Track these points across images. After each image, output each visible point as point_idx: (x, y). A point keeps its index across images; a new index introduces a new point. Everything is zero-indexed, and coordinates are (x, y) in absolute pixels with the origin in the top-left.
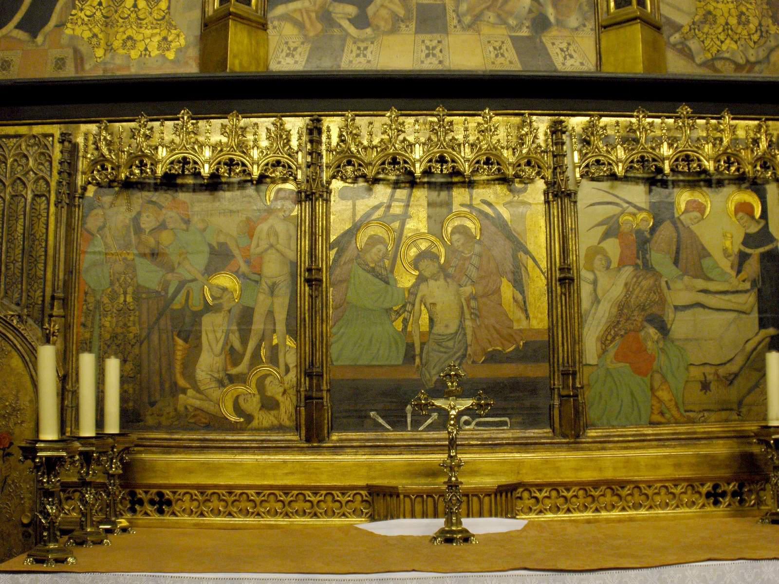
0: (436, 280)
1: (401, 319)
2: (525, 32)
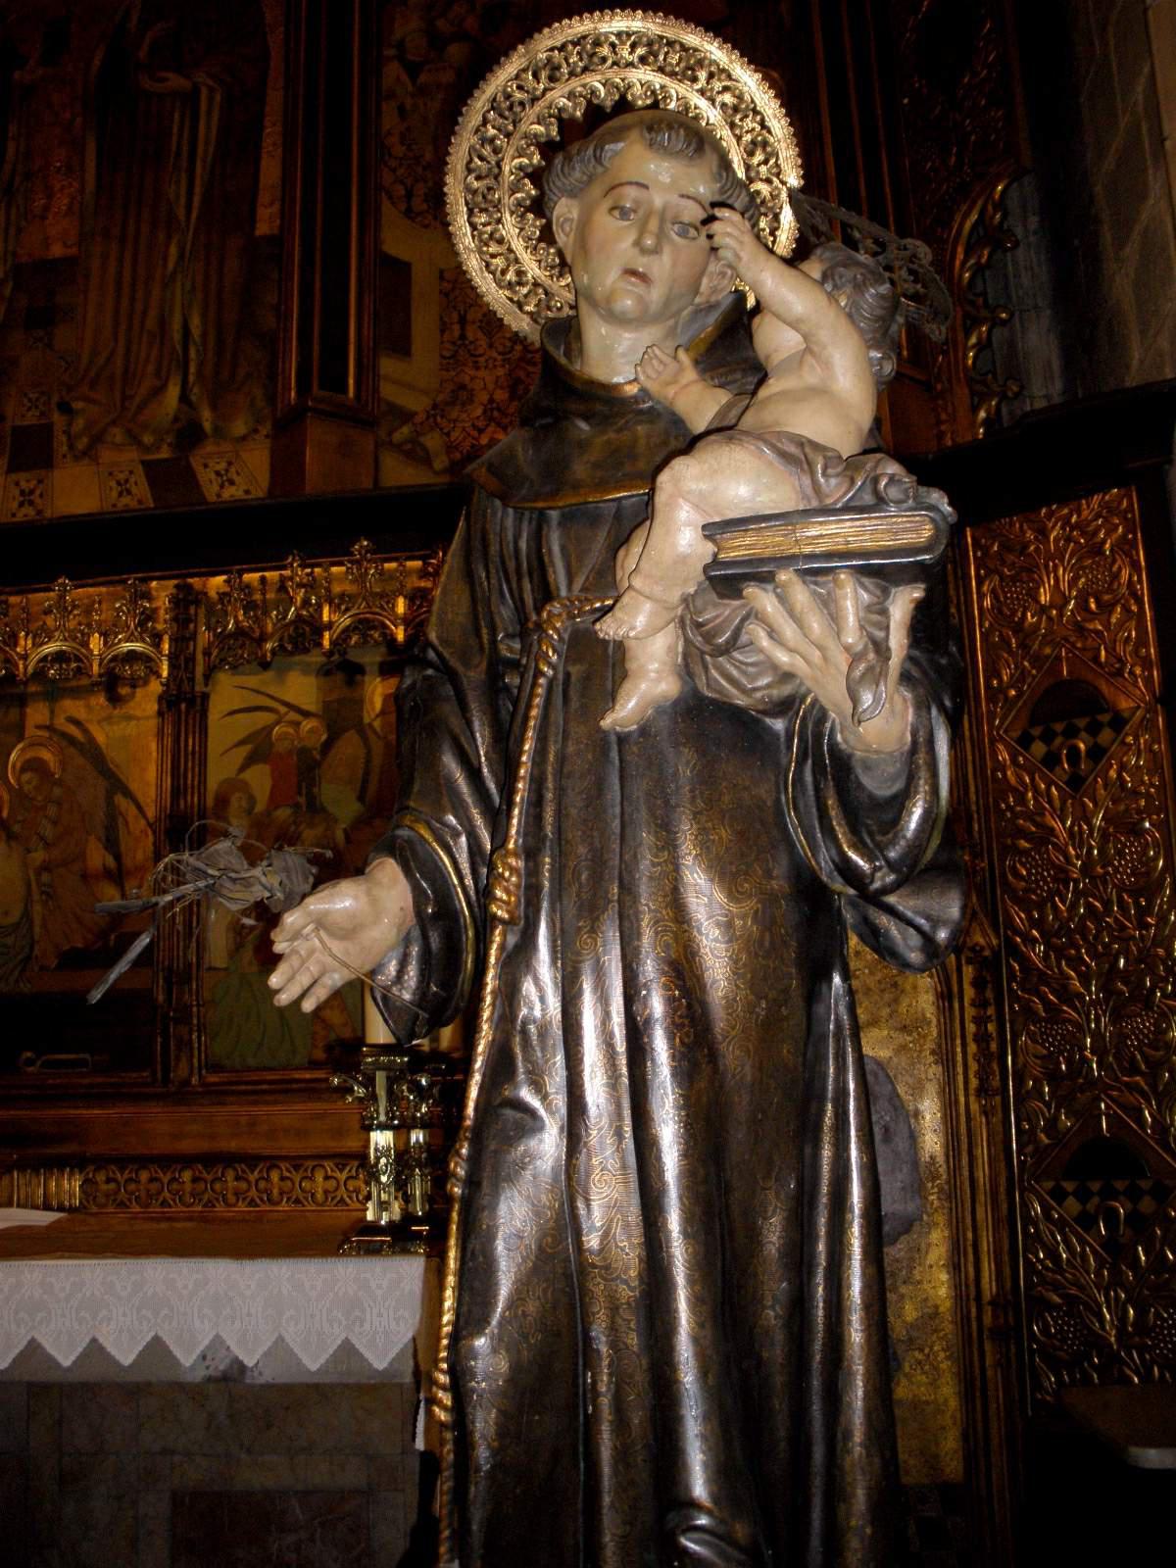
2: (165, 453)
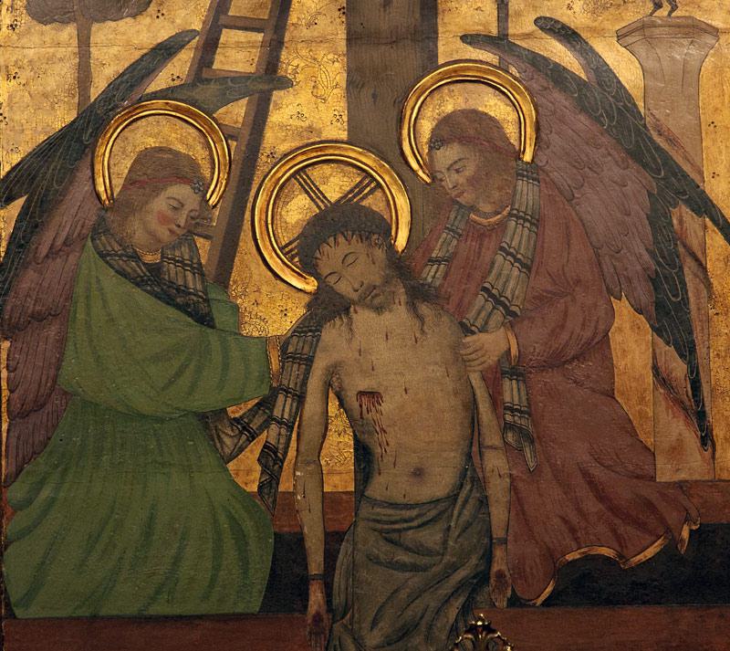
0: (379, 309)
1: (255, 449)
